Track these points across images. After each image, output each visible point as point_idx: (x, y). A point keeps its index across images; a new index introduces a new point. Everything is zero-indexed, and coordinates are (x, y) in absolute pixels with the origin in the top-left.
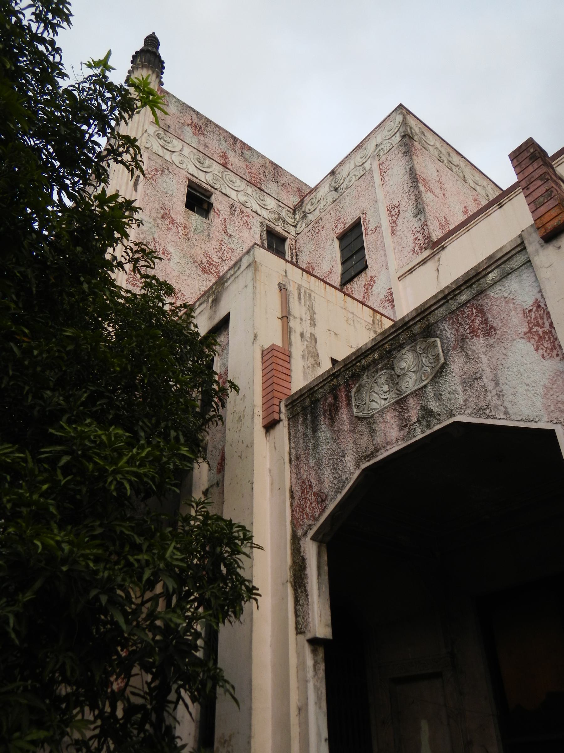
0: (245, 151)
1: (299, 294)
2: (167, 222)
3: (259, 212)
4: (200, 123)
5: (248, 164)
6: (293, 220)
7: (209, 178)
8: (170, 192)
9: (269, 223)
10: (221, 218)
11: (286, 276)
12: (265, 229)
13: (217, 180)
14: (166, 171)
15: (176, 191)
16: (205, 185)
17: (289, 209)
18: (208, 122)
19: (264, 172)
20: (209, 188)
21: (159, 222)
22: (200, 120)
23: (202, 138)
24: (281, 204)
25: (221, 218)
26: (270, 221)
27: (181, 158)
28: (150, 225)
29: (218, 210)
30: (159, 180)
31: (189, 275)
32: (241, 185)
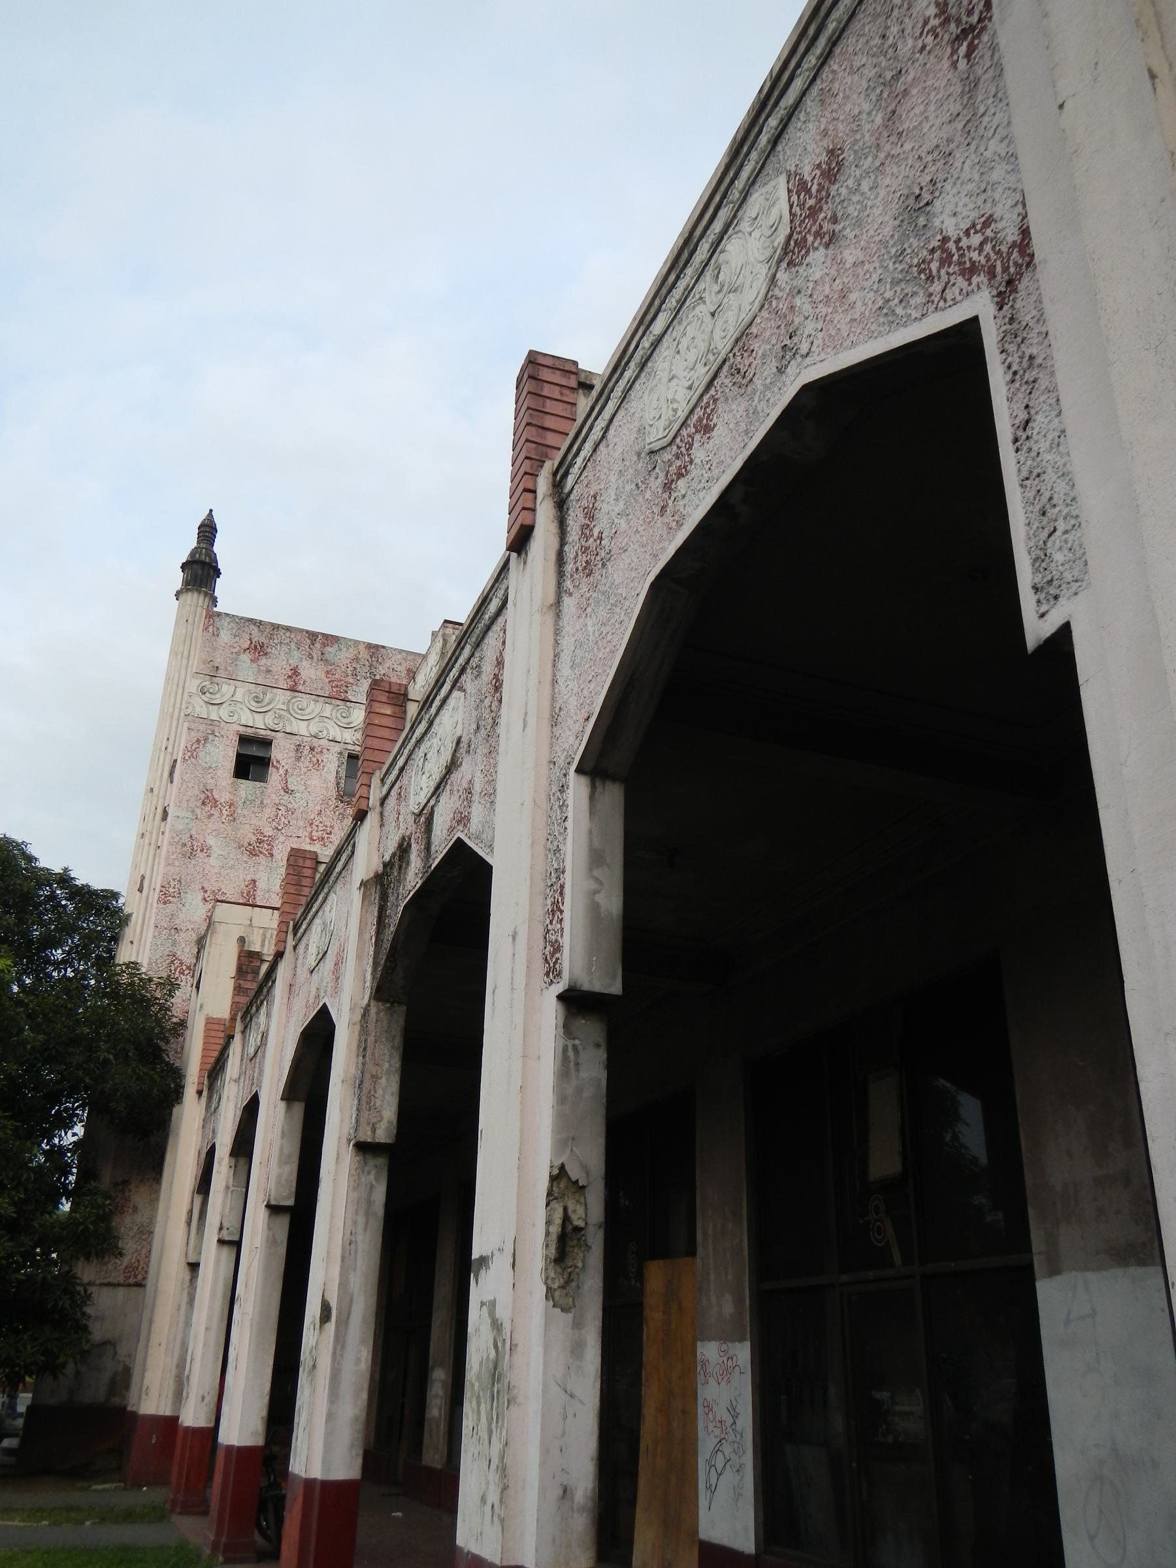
0: (328, 649)
1: (263, 941)
4: (262, 640)
7: (269, 720)
9: (352, 748)
10: (282, 771)
11: (251, 925)
13: (280, 716)
15: (221, 759)
16: (263, 732)
18: (276, 627)
20: (269, 732)
21: (198, 811)
22: (262, 632)
23: (263, 661)
25: (282, 771)
26: (355, 744)
27: (231, 708)
28: (187, 821)
29: (278, 762)
30: (201, 755)
31: (232, 867)
32: (314, 707)
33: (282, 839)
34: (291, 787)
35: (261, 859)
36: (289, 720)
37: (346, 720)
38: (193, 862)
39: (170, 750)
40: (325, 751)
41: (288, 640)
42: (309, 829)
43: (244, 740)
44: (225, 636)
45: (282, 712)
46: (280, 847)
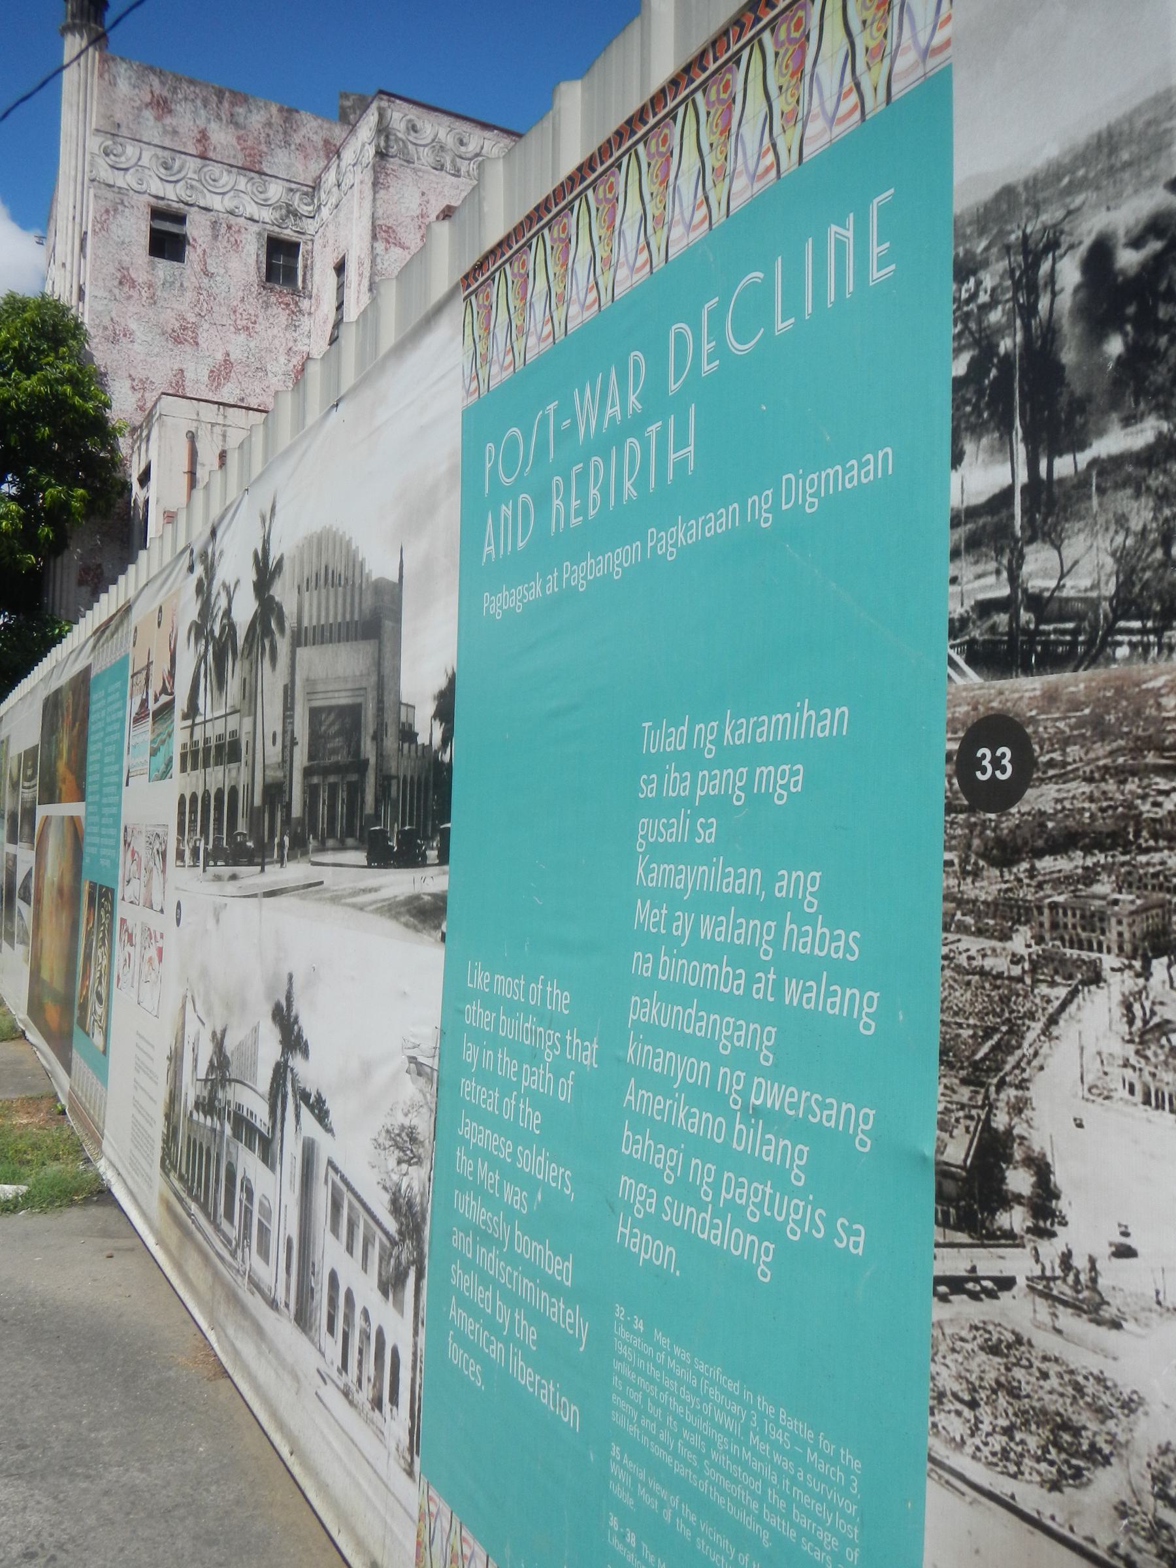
2: (126, 289)
3: (256, 218)
4: (165, 93)
5: (242, 132)
6: (310, 208)
8: (127, 240)
10: (199, 251)
12: (264, 243)
13: (192, 187)
14: (120, 208)
15: (135, 234)
16: (175, 205)
17: (305, 189)
19: (268, 135)
20: (182, 205)
21: (116, 291)
23: (168, 120)
24: (293, 186)
25: (199, 251)
26: (273, 224)
29: (195, 240)
30: (113, 227)
31: (156, 356)
32: (227, 180)
33: (206, 326)
34: (211, 269)
35: (187, 348)
36: (202, 192)
37: (263, 196)
38: (117, 347)
39: (78, 219)
40: (243, 230)
41: (192, 96)
42: (233, 317)
43: (157, 214)
44: (124, 87)
45: (194, 183)
46: (205, 334)
